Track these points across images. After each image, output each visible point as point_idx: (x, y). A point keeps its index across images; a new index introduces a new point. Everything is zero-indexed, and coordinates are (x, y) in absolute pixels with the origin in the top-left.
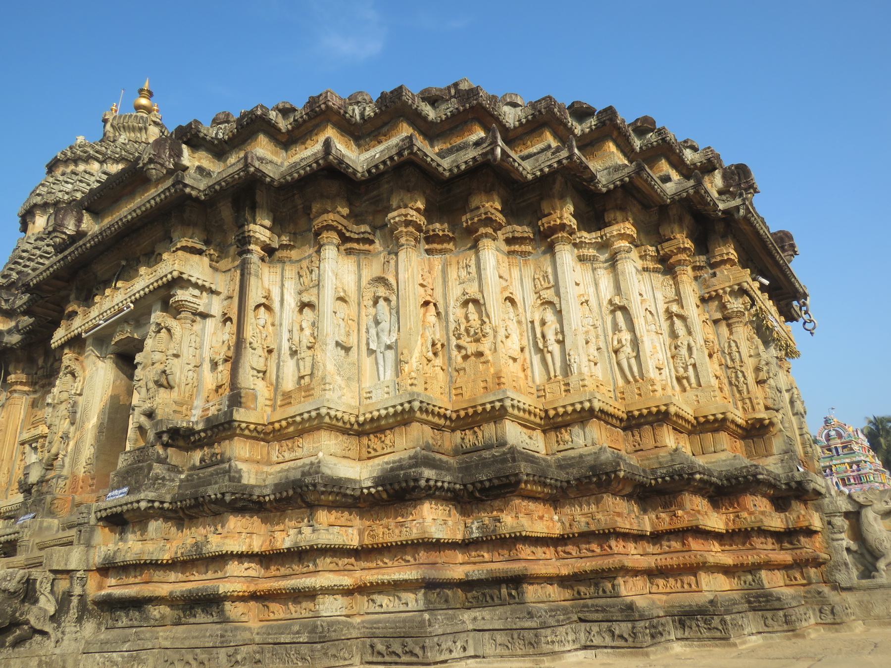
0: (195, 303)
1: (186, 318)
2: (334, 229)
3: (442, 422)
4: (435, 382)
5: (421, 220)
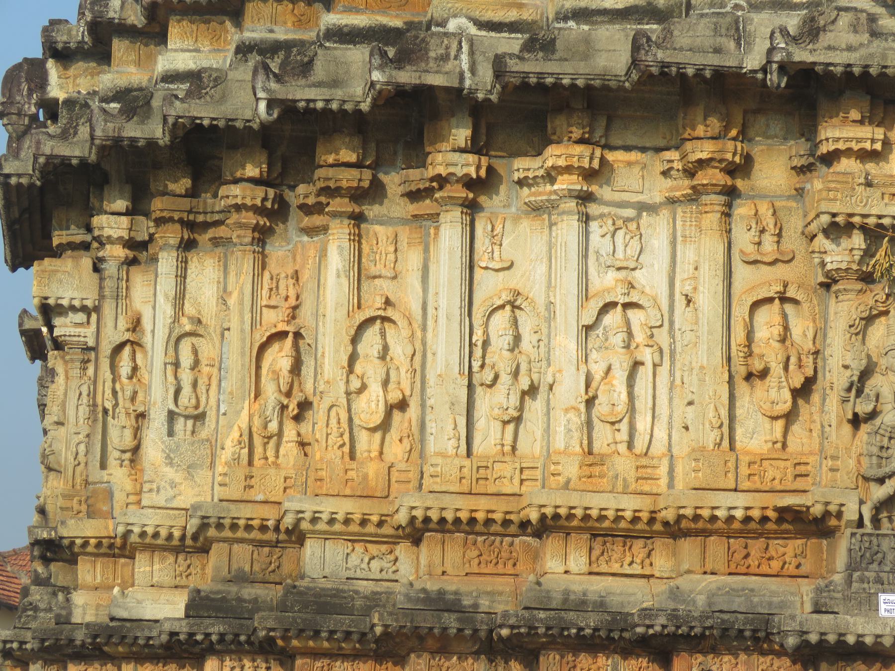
0: (79, 336)
1: (72, 360)
2: (171, 220)
3: (270, 536)
4: (272, 471)
5: (256, 195)
